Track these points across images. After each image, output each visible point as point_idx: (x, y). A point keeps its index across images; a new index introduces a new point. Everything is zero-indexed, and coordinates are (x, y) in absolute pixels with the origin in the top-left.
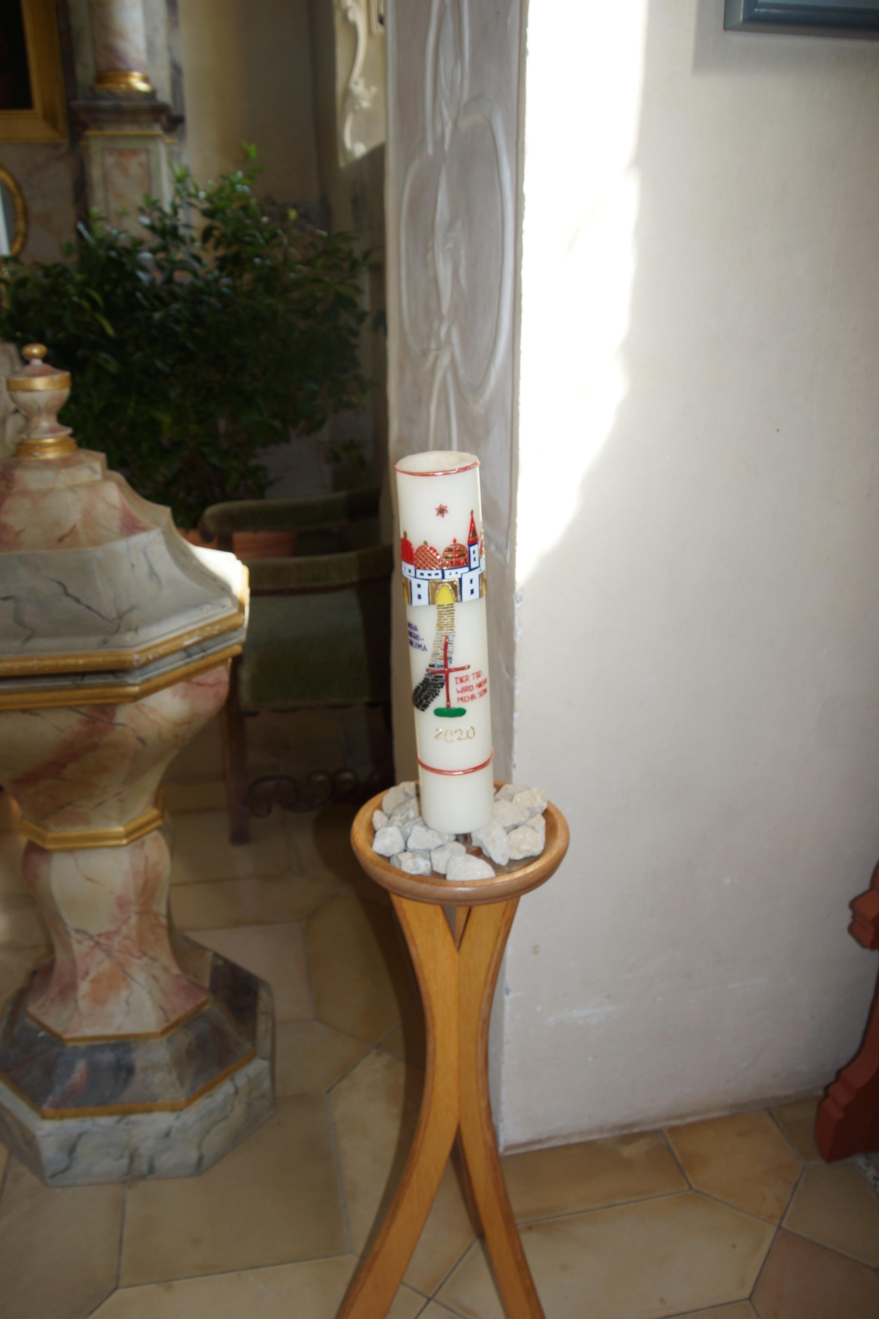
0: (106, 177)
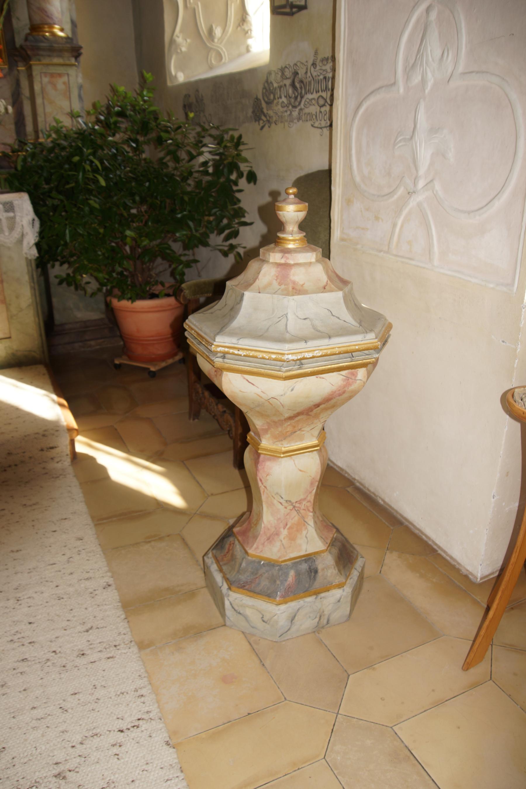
0: (43, 90)
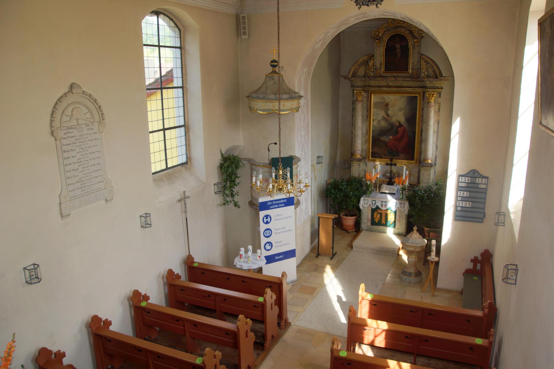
0: (423, 174)
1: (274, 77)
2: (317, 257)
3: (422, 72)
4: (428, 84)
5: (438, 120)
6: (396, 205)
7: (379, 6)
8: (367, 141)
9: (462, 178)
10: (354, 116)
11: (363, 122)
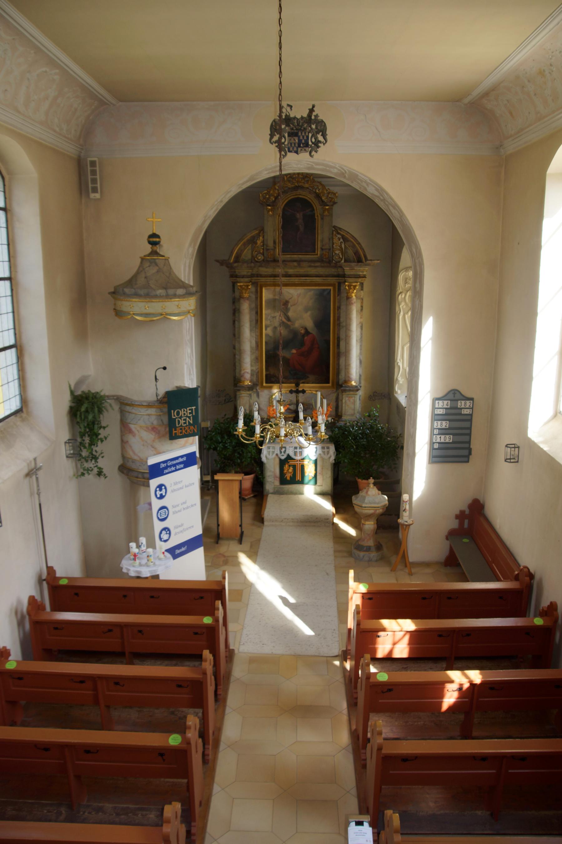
0: (345, 402)
1: (157, 261)
2: (217, 543)
3: (335, 254)
4: (348, 271)
5: (360, 323)
6: (316, 451)
7: (313, 155)
8: (257, 359)
9: (438, 403)
10: (236, 322)
11: (251, 330)
